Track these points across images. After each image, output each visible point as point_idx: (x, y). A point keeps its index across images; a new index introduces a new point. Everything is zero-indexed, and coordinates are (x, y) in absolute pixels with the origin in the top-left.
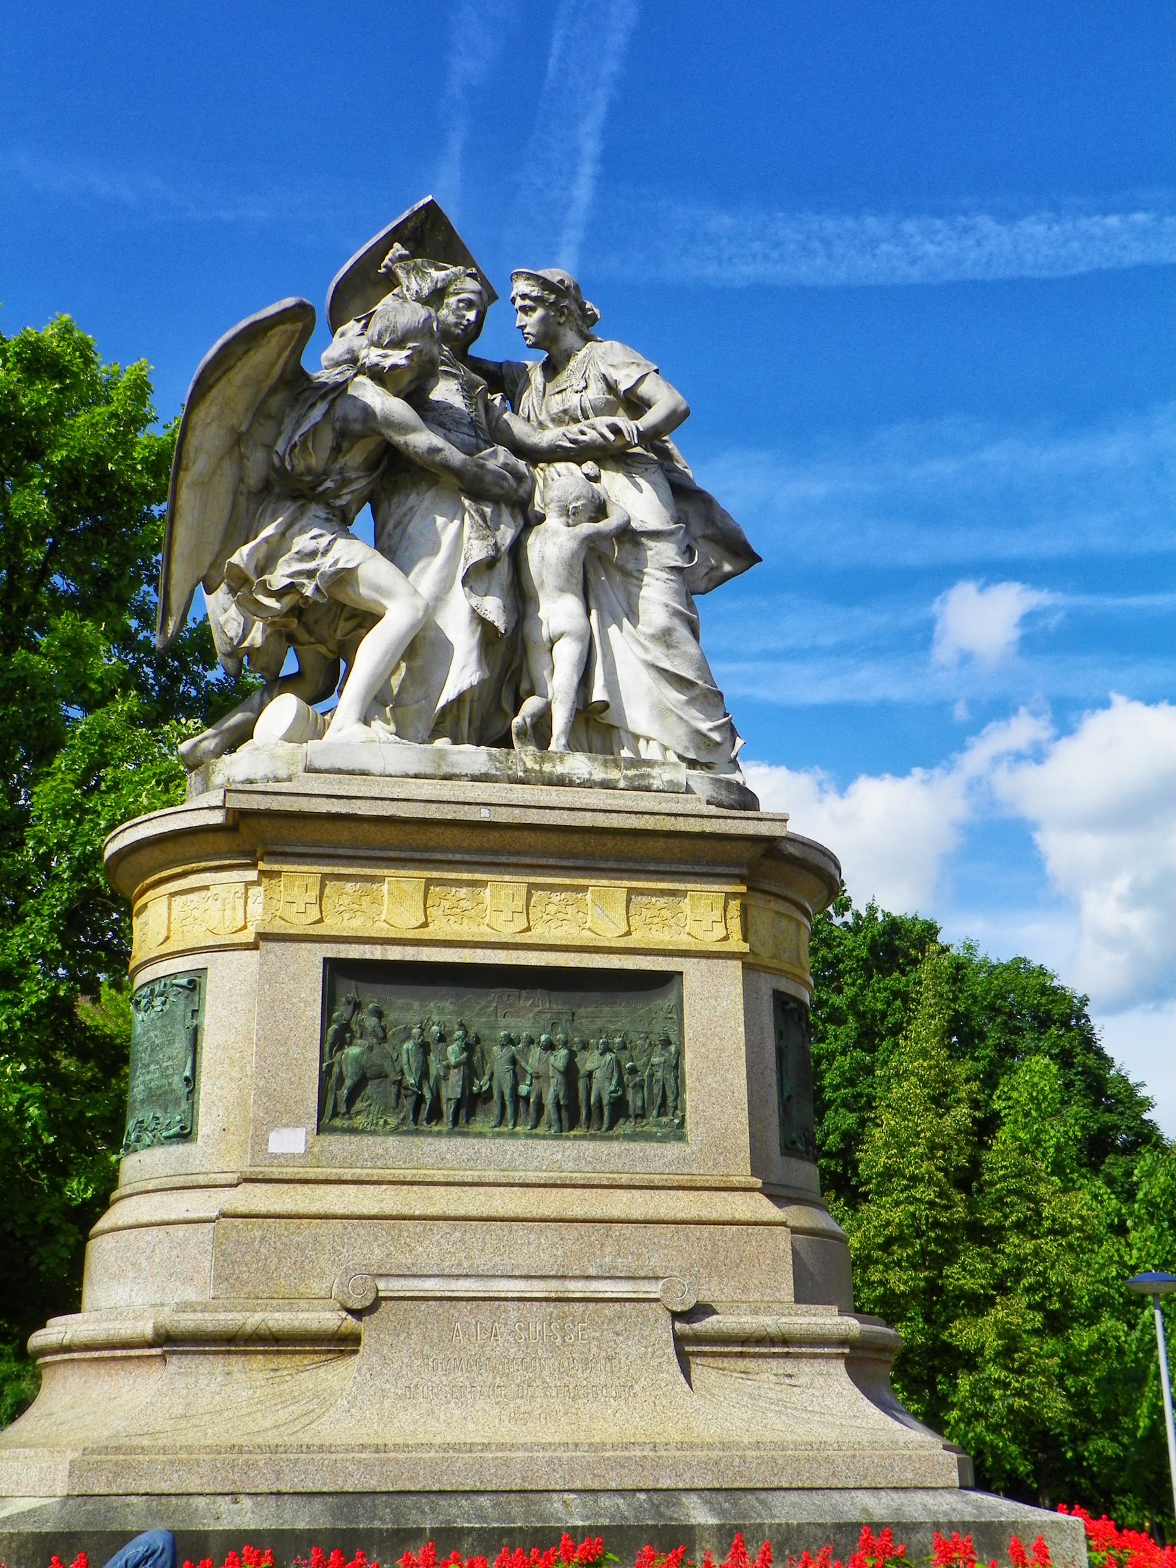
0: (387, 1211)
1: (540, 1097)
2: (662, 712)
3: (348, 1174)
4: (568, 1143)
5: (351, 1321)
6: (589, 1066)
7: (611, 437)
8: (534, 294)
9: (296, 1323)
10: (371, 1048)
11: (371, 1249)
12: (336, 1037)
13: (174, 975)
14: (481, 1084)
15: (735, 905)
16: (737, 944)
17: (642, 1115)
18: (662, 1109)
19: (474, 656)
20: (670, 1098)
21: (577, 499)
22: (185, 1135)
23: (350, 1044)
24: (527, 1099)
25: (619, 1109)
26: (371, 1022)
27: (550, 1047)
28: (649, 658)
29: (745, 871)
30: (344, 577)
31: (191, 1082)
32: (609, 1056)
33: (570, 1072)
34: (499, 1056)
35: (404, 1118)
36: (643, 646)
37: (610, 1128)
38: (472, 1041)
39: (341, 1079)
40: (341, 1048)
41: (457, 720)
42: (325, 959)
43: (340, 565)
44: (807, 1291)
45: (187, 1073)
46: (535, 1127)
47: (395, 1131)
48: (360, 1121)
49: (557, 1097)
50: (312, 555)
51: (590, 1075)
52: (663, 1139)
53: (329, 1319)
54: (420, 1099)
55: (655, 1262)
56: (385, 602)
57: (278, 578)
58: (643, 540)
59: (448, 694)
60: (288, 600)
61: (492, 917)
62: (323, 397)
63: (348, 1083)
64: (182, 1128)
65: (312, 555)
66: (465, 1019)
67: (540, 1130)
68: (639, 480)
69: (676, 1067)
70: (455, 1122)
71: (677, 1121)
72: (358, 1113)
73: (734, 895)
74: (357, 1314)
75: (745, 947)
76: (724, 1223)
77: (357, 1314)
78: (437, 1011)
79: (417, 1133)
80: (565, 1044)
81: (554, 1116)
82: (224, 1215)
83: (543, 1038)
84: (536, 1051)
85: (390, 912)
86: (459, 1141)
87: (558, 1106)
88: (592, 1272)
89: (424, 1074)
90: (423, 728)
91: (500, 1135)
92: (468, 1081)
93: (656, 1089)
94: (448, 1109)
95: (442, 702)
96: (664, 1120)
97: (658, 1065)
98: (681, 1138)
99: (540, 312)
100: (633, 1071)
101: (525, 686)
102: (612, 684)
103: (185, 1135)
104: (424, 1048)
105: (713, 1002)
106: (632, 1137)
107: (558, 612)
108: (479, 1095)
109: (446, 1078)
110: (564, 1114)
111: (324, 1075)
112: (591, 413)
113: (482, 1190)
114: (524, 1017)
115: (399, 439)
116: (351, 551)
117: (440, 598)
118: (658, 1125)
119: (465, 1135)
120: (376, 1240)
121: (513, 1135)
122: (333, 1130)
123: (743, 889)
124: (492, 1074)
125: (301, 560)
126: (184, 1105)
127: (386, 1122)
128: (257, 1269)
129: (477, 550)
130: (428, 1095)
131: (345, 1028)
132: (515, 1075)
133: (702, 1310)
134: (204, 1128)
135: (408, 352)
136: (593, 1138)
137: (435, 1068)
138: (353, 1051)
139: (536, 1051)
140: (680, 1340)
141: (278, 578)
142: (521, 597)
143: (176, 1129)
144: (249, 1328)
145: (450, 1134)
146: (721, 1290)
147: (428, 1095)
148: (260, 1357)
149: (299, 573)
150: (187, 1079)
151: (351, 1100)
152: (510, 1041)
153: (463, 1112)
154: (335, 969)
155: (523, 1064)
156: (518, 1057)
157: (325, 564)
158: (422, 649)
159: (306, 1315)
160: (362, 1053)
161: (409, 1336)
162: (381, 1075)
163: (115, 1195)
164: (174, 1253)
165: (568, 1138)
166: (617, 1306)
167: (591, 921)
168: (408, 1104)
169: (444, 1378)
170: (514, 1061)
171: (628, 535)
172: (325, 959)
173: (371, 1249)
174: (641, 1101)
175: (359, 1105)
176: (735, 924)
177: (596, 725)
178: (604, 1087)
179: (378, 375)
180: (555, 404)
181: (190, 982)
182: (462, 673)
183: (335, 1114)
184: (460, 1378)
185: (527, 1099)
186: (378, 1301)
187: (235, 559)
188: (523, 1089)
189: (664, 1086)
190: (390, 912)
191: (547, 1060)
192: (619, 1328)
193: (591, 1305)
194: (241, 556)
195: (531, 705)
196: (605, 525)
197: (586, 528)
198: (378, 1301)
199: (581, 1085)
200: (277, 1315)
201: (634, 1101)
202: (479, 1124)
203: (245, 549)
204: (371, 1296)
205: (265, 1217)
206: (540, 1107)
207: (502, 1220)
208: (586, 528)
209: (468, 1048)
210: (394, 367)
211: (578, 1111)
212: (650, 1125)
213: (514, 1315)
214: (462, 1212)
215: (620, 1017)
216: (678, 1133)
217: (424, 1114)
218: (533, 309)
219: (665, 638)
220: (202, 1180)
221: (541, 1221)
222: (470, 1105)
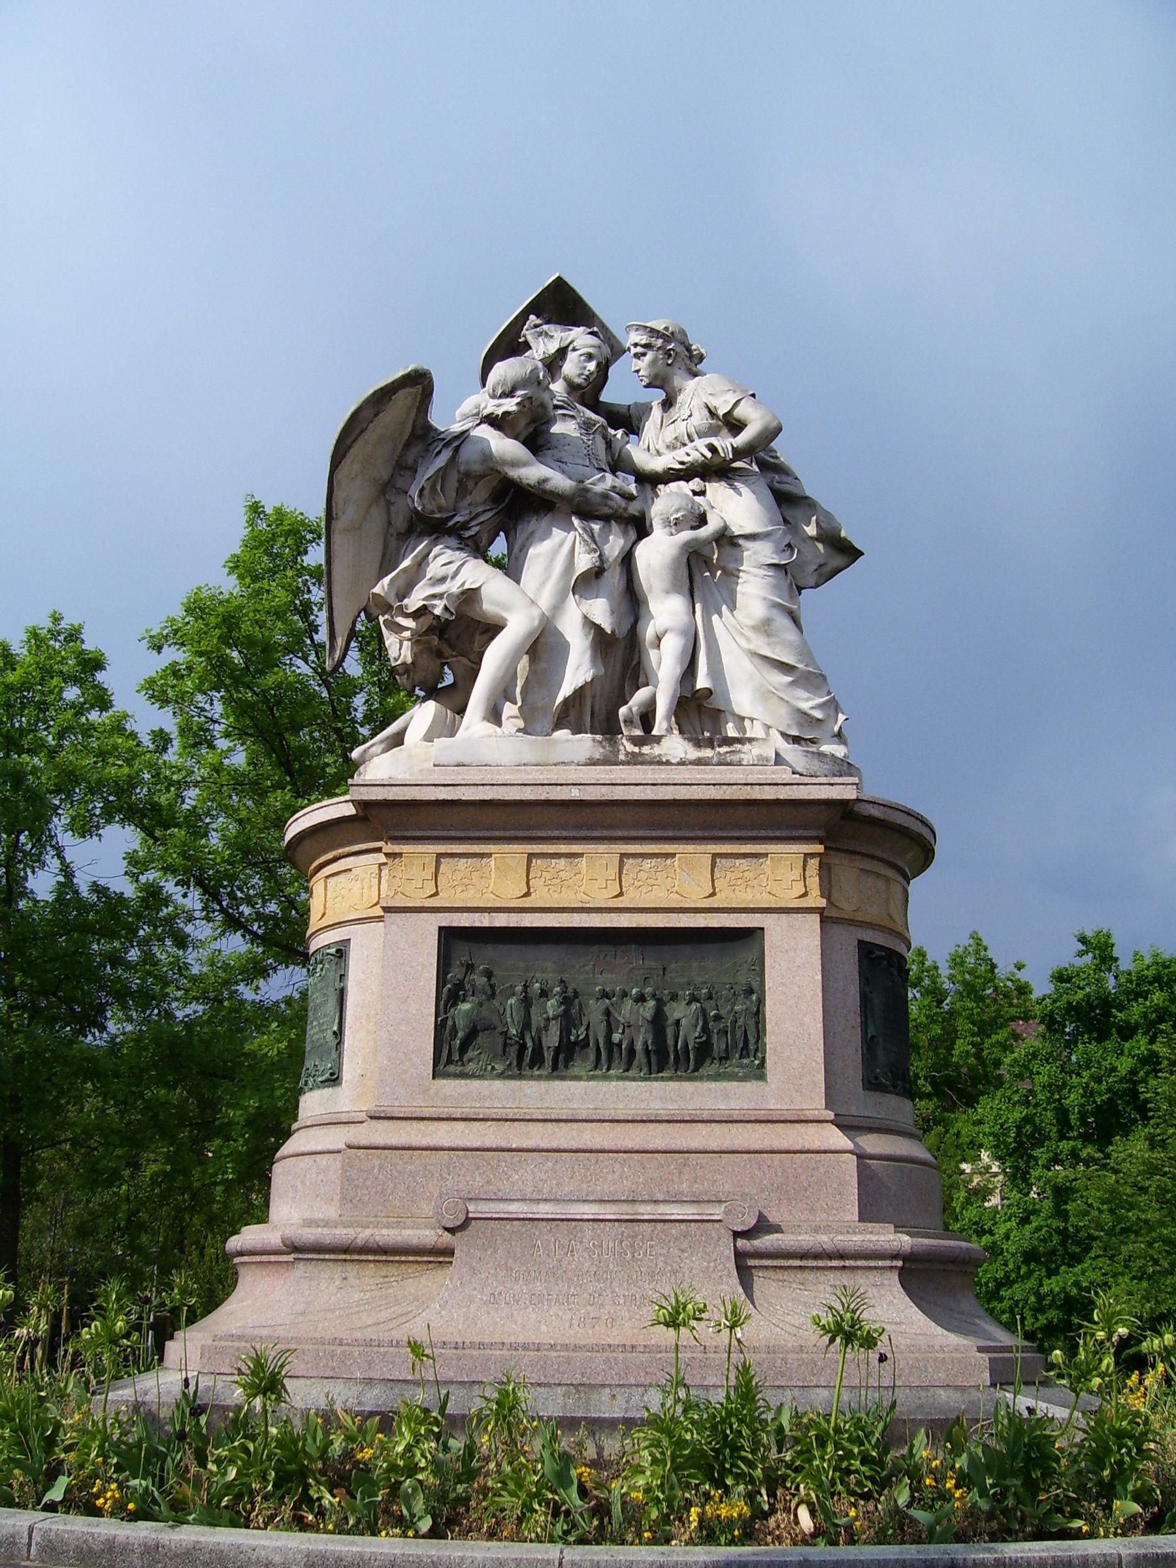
0: (488, 1144)
2: (765, 695)
4: (656, 1084)
6: (677, 1015)
7: (709, 455)
8: (643, 342)
9: (399, 1238)
10: (481, 1004)
11: (471, 1177)
12: (449, 994)
13: (328, 946)
15: (814, 863)
17: (725, 1058)
19: (588, 656)
20: (752, 1040)
21: (677, 511)
22: (334, 1080)
23: (463, 1001)
24: (620, 1045)
25: (704, 1052)
26: (481, 981)
27: (641, 999)
28: (752, 647)
29: (821, 833)
30: (470, 596)
31: (339, 1034)
32: (694, 1006)
33: (658, 1021)
34: (594, 1011)
35: (510, 1065)
36: (745, 636)
37: (696, 1070)
38: (570, 993)
39: (454, 1030)
40: (455, 1004)
43: (466, 587)
44: (868, 1213)
45: (335, 1028)
46: (627, 1070)
47: (502, 1076)
48: (471, 1067)
49: (646, 1043)
50: (443, 580)
51: (677, 1023)
52: (744, 1079)
53: (429, 1236)
55: (725, 1186)
56: (505, 615)
57: (414, 601)
58: (741, 542)
59: (566, 690)
60: (426, 621)
61: (586, 886)
62: (447, 445)
63: (460, 1034)
64: (332, 1074)
65: (443, 580)
66: (566, 976)
67: (630, 1073)
69: (758, 1014)
70: (555, 1067)
71: (757, 1062)
72: (470, 1060)
73: (812, 855)
75: (823, 903)
76: (794, 1152)
78: (545, 968)
79: (520, 1077)
80: (654, 995)
81: (644, 1060)
82: (350, 1147)
83: (634, 991)
84: (629, 1003)
85: (493, 884)
86: (557, 1084)
87: (647, 1052)
88: (660, 1197)
89: (526, 1025)
90: (548, 721)
91: (593, 1078)
92: (565, 1031)
93: (739, 1034)
94: (548, 1056)
95: (560, 699)
96: (745, 1061)
97: (741, 1013)
99: (650, 356)
100: (718, 1018)
101: (642, 679)
102: (716, 670)
103: (334, 1080)
104: (526, 1002)
105: (792, 953)
106: (717, 1077)
107: (666, 611)
108: (576, 1043)
109: (546, 1028)
110: (653, 1058)
111: (439, 1028)
112: (695, 437)
113: (575, 1125)
114: (597, 975)
115: (514, 473)
117: (558, 606)
118: (741, 1066)
119: (563, 1078)
120: (477, 1169)
121: (605, 1078)
122: (447, 1076)
123: (820, 848)
124: (588, 1025)
125: (433, 585)
126: (334, 1055)
127: (493, 1068)
128: (377, 1192)
131: (460, 986)
132: (609, 1023)
133: (763, 1226)
134: (347, 1074)
135: (519, 400)
137: (537, 1020)
138: (465, 1007)
139: (629, 1003)
140: (740, 1256)
141: (414, 601)
142: (632, 600)
143: (327, 1076)
144: (360, 1242)
145: (549, 1078)
146: (790, 1211)
147: (530, 1044)
148: (372, 1265)
149: (434, 596)
150: (334, 1033)
151: (463, 1049)
152: (605, 995)
153: (561, 1057)
154: (448, 935)
155: (616, 1015)
156: (611, 1009)
157: (453, 587)
159: (408, 1232)
160: (472, 1009)
161: (496, 1252)
162: (490, 1028)
164: (320, 1178)
165: (656, 1079)
166: (683, 1226)
167: (675, 885)
168: (513, 1051)
169: (524, 1287)
170: (608, 1013)
171: (726, 539)
173: (471, 1177)
174: (729, 1043)
175: (471, 1054)
176: (814, 882)
177: (699, 711)
178: (690, 1034)
179: (493, 421)
180: (669, 434)
181: (338, 951)
182: (578, 671)
183: (450, 1061)
184: (539, 1287)
185: (620, 1045)
186: (468, 1221)
187: (377, 590)
188: (616, 1037)
189: (746, 1031)
190: (493, 884)
191: (638, 1011)
192: (685, 1245)
193: (659, 1226)
194: (382, 587)
195: (642, 695)
196: (705, 532)
197: (686, 535)
198: (468, 1221)
199: (670, 1032)
200: (384, 1232)
201: (719, 1045)
202: (577, 1068)
203: (386, 580)
204: (462, 1217)
205: (384, 1148)
206: (632, 1051)
207: (591, 1151)
208: (686, 535)
209: (567, 1001)
210: (506, 413)
211: (664, 1057)
212: (731, 1067)
213: (588, 1234)
214: (554, 1145)
215: (705, 970)
216: (759, 1073)
217: (527, 1060)
218: (644, 354)
219: (765, 627)
220: (344, 1118)
221: (625, 1152)
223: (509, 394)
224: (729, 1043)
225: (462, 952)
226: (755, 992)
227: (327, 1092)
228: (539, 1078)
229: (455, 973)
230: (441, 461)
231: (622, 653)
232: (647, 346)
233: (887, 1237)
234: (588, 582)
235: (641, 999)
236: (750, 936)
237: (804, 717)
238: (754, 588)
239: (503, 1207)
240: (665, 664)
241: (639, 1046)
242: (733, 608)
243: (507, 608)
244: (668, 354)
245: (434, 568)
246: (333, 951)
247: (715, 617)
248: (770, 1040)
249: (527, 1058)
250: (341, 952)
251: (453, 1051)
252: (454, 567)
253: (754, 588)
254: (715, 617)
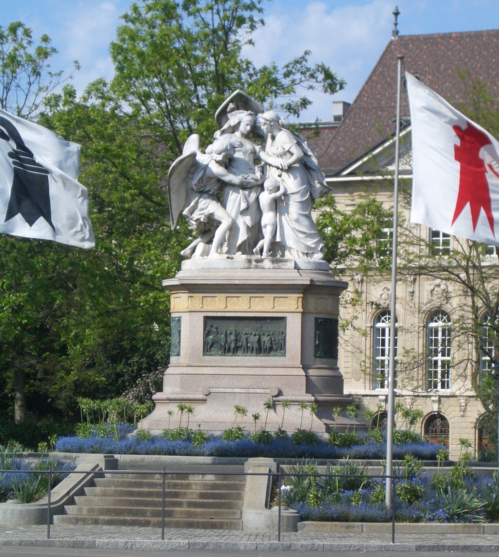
0: (216, 373)
1: (253, 347)
2: (297, 241)
3: (209, 365)
5: (205, 397)
6: (264, 339)
12: (207, 334)
14: (239, 344)
15: (300, 300)
17: (276, 350)
18: (281, 349)
19: (245, 232)
25: (271, 349)
27: (255, 335)
31: (179, 342)
32: (269, 337)
33: (259, 340)
34: (244, 338)
38: (237, 333)
39: (208, 343)
41: (245, 246)
42: (204, 317)
47: (220, 355)
48: (213, 353)
50: (203, 209)
52: (281, 356)
53: (201, 396)
54: (225, 348)
56: (222, 221)
59: (239, 242)
60: (198, 221)
61: (240, 305)
63: (210, 344)
65: (203, 209)
67: (253, 354)
70: (234, 352)
73: (300, 297)
74: (206, 395)
77: (206, 395)
78: (232, 327)
79: (224, 356)
86: (234, 357)
87: (257, 349)
89: (226, 342)
90: (235, 250)
91: (243, 356)
92: (236, 344)
94: (232, 350)
100: (274, 340)
103: (178, 355)
104: (226, 336)
106: (274, 356)
107: (268, 218)
119: (235, 356)
121: (246, 356)
122: (206, 355)
130: (227, 347)
131: (209, 331)
134: (182, 354)
136: (264, 356)
137: (229, 340)
138: (211, 337)
139: (252, 336)
144: (185, 398)
145: (232, 356)
147: (227, 347)
149: (201, 214)
151: (211, 348)
152: (246, 334)
154: (206, 318)
157: (206, 212)
158: (233, 229)
162: (217, 342)
163: (169, 365)
168: (223, 349)
170: (247, 339)
172: (204, 317)
175: (212, 349)
176: (300, 304)
177: (277, 247)
178: (268, 345)
182: (242, 236)
183: (207, 351)
184: (226, 408)
186: (210, 393)
188: (249, 345)
190: (218, 305)
197: (274, 195)
198: (210, 393)
201: (275, 347)
202: (240, 353)
209: (236, 336)
211: (261, 349)
212: (277, 353)
216: (284, 355)
219: (297, 221)
220: (181, 365)
223: (220, 154)
224: (276, 347)
225: (210, 322)
226: (284, 333)
227: (177, 357)
228: (229, 356)
229: (208, 328)
230: (200, 175)
231: (256, 231)
235: (255, 335)
236: (283, 319)
238: (294, 208)
239: (218, 389)
241: (254, 348)
243: (222, 218)
244: (271, 126)
245: (201, 206)
246: (177, 319)
248: (287, 346)
249: (227, 350)
250: (179, 321)
251: (208, 348)
252: (206, 205)
253: (294, 208)
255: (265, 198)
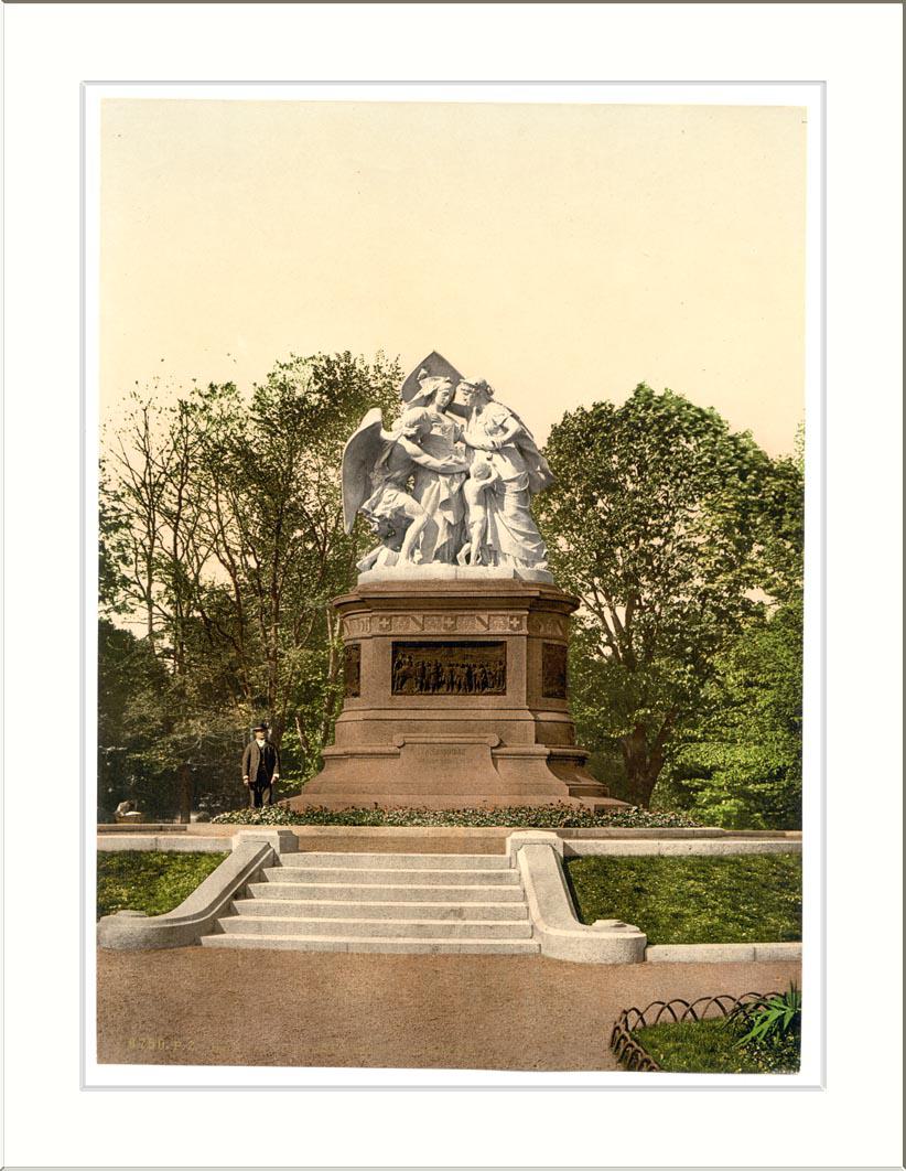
16: (525, 631)
25: (485, 684)
50: (388, 503)
53: (393, 749)
56: (415, 518)
68: (507, 459)
95: (438, 546)
98: (505, 694)
107: (476, 514)
115: (416, 459)
116: (404, 499)
117: (434, 511)
122: (397, 694)
129: (444, 495)
137: (427, 672)
141: (378, 512)
142: (463, 507)
152: (450, 665)
154: (397, 646)
157: (394, 506)
177: (489, 553)
179: (408, 438)
182: (442, 538)
195: (467, 546)
202: (444, 689)
209: (438, 668)
222: (438, 685)
223: (412, 426)
231: (460, 530)
232: (469, 391)
233: (543, 749)
234: (445, 505)
237: (527, 552)
238: (510, 502)
240: (475, 532)
242: (503, 510)
245: (385, 497)
247: (495, 514)
251: (400, 683)
252: (392, 497)
253: (510, 502)
254: (495, 514)
255: (472, 487)
